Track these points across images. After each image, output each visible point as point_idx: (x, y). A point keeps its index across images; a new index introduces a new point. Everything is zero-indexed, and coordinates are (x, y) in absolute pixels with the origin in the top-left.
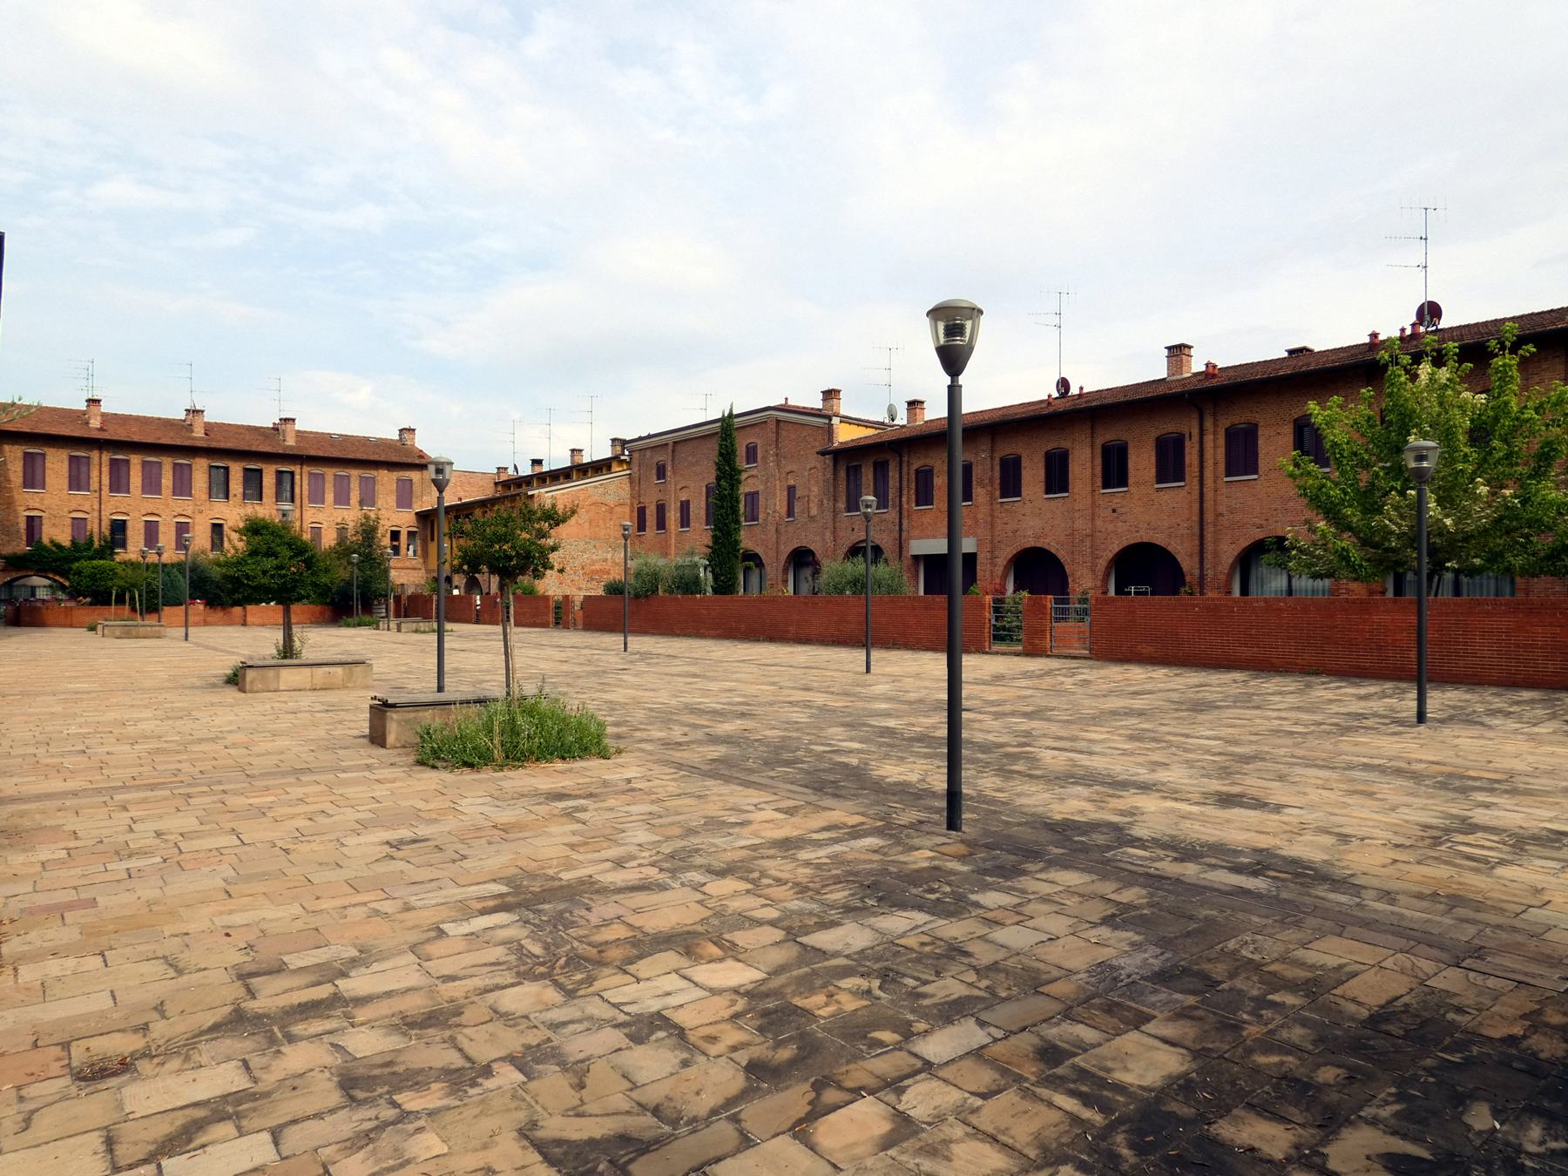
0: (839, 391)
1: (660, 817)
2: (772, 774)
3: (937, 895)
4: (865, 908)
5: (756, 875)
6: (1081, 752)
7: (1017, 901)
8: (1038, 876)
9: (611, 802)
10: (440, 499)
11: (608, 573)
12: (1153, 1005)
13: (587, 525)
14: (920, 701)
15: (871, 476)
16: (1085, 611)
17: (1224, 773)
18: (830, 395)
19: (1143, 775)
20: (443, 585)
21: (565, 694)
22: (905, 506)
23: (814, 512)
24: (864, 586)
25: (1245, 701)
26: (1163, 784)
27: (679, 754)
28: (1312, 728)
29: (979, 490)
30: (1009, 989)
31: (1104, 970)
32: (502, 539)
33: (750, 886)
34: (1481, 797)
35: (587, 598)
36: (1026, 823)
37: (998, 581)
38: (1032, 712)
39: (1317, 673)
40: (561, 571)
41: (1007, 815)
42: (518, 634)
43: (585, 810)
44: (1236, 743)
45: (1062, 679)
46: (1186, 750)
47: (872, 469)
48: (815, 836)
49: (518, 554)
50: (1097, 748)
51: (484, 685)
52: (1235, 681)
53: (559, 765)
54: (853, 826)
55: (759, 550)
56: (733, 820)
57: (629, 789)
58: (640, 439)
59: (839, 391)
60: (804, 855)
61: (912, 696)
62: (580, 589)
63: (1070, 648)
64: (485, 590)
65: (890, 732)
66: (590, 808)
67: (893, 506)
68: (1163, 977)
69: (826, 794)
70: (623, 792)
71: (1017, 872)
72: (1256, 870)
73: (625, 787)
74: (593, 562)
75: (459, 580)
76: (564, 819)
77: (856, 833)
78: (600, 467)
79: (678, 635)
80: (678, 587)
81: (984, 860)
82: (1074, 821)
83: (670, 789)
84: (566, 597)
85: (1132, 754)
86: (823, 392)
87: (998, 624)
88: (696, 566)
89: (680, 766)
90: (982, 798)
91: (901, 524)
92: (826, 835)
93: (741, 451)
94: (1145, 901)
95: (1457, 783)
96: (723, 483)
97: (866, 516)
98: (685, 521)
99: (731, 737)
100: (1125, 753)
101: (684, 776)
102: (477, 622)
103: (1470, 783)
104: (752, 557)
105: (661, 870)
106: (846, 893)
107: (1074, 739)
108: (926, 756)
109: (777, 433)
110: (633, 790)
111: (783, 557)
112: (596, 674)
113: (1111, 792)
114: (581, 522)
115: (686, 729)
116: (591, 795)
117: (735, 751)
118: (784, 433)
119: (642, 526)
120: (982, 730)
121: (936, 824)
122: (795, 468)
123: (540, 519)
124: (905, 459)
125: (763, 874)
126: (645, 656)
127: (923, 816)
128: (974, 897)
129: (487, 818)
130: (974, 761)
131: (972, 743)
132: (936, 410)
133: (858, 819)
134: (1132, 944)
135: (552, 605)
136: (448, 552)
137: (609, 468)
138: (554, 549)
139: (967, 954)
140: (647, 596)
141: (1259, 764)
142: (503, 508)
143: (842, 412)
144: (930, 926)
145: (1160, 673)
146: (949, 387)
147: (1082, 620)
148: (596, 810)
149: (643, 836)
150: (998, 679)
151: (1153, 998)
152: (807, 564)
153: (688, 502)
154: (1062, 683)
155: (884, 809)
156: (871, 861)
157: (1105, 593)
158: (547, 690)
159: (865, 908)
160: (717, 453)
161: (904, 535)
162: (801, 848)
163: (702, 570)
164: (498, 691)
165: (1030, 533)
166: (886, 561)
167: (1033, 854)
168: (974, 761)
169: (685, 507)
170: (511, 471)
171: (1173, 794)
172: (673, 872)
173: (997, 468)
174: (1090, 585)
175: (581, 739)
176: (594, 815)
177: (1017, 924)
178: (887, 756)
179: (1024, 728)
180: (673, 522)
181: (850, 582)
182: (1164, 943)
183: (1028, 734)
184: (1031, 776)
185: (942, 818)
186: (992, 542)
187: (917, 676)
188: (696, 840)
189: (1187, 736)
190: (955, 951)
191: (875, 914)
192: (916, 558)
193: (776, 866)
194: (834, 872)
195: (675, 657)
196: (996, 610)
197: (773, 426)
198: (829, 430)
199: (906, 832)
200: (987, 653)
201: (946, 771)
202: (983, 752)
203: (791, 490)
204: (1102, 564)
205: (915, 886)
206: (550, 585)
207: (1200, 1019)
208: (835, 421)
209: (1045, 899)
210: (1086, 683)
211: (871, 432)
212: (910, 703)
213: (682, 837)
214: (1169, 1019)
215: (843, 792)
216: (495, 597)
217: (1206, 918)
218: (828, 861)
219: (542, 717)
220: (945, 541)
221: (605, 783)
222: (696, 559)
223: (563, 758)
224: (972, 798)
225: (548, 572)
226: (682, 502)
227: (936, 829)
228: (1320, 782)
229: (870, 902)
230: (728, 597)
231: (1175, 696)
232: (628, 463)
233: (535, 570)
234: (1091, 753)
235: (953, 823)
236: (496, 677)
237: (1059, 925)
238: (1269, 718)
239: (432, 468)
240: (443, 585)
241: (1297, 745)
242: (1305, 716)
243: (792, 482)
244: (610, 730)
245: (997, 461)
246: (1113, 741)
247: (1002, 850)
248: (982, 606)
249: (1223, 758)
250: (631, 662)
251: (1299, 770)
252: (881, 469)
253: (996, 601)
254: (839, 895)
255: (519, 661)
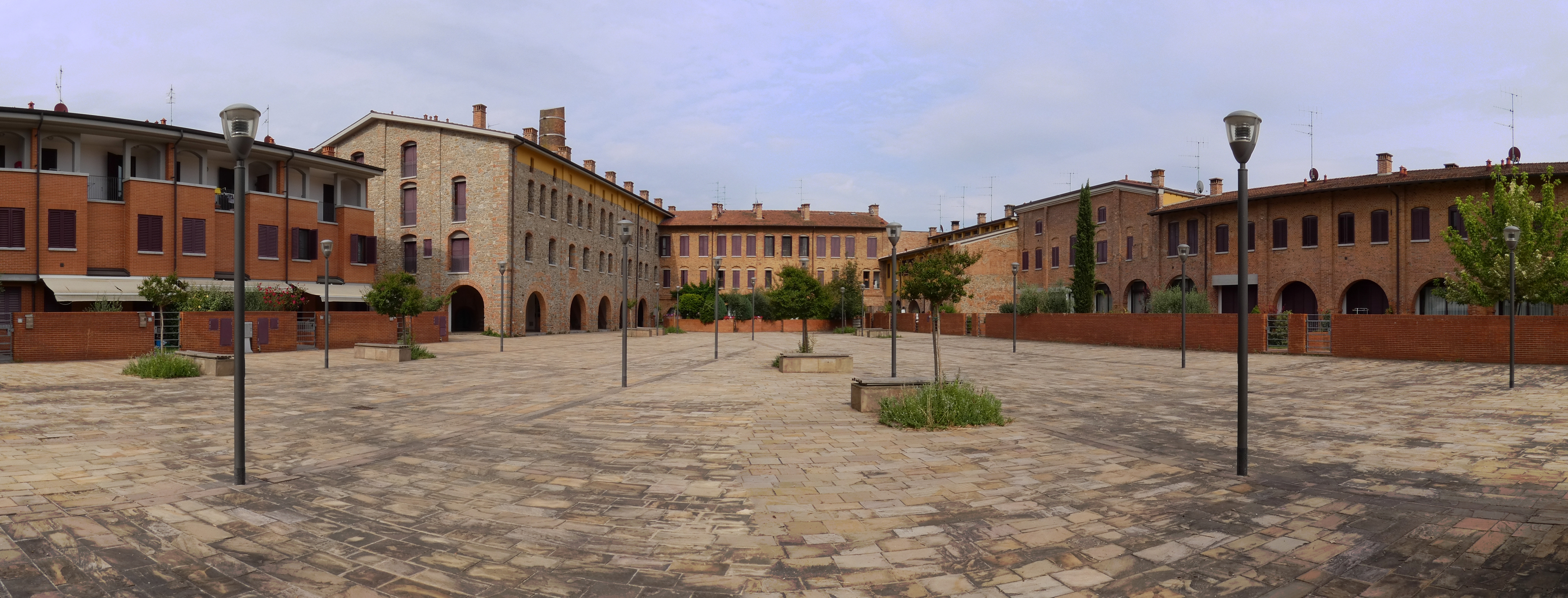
0: (1163, 171)
1: (1038, 467)
2: (1116, 438)
3: (1231, 520)
4: (1181, 531)
5: (1105, 509)
6: (1325, 418)
7: (1284, 520)
8: (1298, 502)
9: (1005, 456)
10: (894, 250)
11: (1003, 298)
12: (1368, 579)
13: (988, 265)
14: (1219, 387)
15: (1185, 230)
16: (1328, 325)
17: (1411, 426)
18: (1157, 173)
19: (1364, 430)
20: (896, 307)
21: (973, 381)
22: (1209, 252)
23: (1146, 255)
24: (1181, 307)
25: (1422, 380)
26: (1375, 436)
27: (1051, 424)
28: (1458, 394)
29: (1259, 241)
30: (1278, 580)
31: (1339, 561)
32: (932, 275)
33: (1100, 517)
34: (1538, 426)
35: (988, 315)
36: (1290, 468)
37: (1272, 304)
38: (1294, 393)
39: (1461, 361)
40: (971, 297)
41: (1278, 463)
42: (944, 340)
43: (987, 460)
44: (1417, 406)
45: (1312, 369)
46: (1389, 413)
47: (1186, 226)
48: (1146, 482)
49: (943, 286)
50: (1335, 415)
51: (921, 373)
52: (1417, 368)
53: (970, 429)
54: (1172, 475)
55: (1107, 282)
56: (1088, 470)
57: (1016, 447)
58: (1025, 205)
59: (1163, 171)
60: (1138, 495)
61: (1214, 383)
62: (984, 309)
63: (1319, 349)
64: (922, 310)
65: (1198, 408)
66: (991, 459)
67: (1201, 252)
68: (1374, 560)
69: (1154, 452)
70: (1013, 449)
71: (1285, 501)
72: (1426, 485)
73: (1013, 445)
74: (993, 291)
75: (905, 303)
76: (973, 466)
77: (1175, 479)
78: (997, 225)
79: (1051, 341)
80: (1051, 308)
81: (1262, 494)
82: (1320, 464)
83: (1045, 448)
84: (974, 315)
85: (1357, 417)
86: (1152, 172)
87: (1272, 333)
88: (1063, 293)
89: (1052, 432)
90: (1261, 452)
91: (1206, 264)
92: (1154, 481)
93: (1095, 213)
94: (1363, 512)
95: (1528, 420)
96: (1082, 235)
97: (1182, 257)
98: (1055, 262)
99: (1087, 412)
100: (1352, 417)
101: (1055, 439)
102: (917, 331)
103: (1534, 419)
104: (1102, 286)
105: (1039, 504)
106: (1168, 521)
107: (1320, 409)
108: (1223, 425)
109: (1120, 200)
110: (1019, 448)
111: (1124, 287)
112: (994, 367)
113: (1344, 443)
114: (984, 263)
115: (1056, 407)
116: (991, 451)
117: (1091, 423)
118: (1125, 200)
119: (1025, 265)
120: (1261, 406)
121: (1230, 471)
122: (1132, 224)
123: (957, 262)
124: (1209, 219)
125: (1110, 508)
126: (1028, 355)
127: (1220, 466)
128: (1255, 520)
129: (923, 462)
130: (1255, 427)
131: (1254, 415)
132: (1230, 186)
133: (1176, 469)
134: (1356, 541)
135: (965, 320)
136: (898, 284)
137: (1003, 226)
138: (966, 282)
139: (1250, 559)
140: (1029, 314)
141: (1430, 419)
142: (933, 255)
143: (1166, 186)
144: (1225, 542)
145: (1374, 364)
146: (1239, 170)
147: (1326, 330)
148: (994, 461)
149: (1026, 480)
150: (1272, 371)
151: (1368, 574)
152: (1141, 292)
153: (1057, 248)
154: (1313, 372)
155: (1194, 462)
156: (1185, 499)
157: (1340, 312)
158: (961, 378)
159: (1181, 531)
160: (1077, 214)
161: (1208, 271)
162: (1136, 490)
163: (1067, 296)
164: (931, 378)
165: (1293, 271)
166: (1196, 290)
167: (1294, 488)
168: (1255, 427)
169: (1055, 252)
170: (938, 230)
171: (1382, 442)
172: (1047, 506)
173: (1271, 227)
174: (1331, 307)
175: (984, 411)
176: (993, 464)
177: (1284, 536)
178: (1196, 425)
179: (1289, 403)
180: (1047, 263)
181: (1170, 305)
182: (1375, 538)
183: (1291, 407)
184: (1293, 436)
185: (1234, 467)
186: (1268, 278)
187: (1217, 369)
188: (1062, 484)
189: (1390, 404)
190: (1243, 557)
191: (1188, 535)
192: (1216, 287)
193: (1119, 503)
194: (1159, 507)
195: (1048, 356)
196: (1271, 324)
197: (1117, 195)
198: (1157, 198)
199: (1209, 477)
200: (1264, 353)
201: (1236, 434)
202: (1262, 421)
203: (1130, 240)
204: (1339, 293)
205: (1216, 515)
206: (964, 307)
207: (1396, 582)
208: (1161, 191)
209: (1302, 518)
210: (1328, 372)
211: (1186, 200)
212: (1212, 388)
213: (1053, 482)
214: (1378, 586)
215: (1166, 451)
216: (928, 315)
217: (1400, 518)
218: (1155, 499)
219: (959, 396)
220: (1236, 276)
221: (1001, 443)
222: (1063, 288)
223: (973, 425)
224: (1254, 453)
225: (963, 298)
226: (1053, 249)
227: (1230, 475)
228: (1462, 427)
229: (1184, 527)
230: (1085, 315)
231: (1382, 379)
232: (1017, 222)
233: (954, 296)
234: (1331, 418)
235: (1241, 470)
236: (929, 368)
237: (1310, 534)
238: (1435, 390)
239: (889, 230)
240: (896, 307)
241: (1450, 405)
242: (1455, 388)
243: (1130, 234)
244: (1004, 406)
245: (1271, 222)
246: (1345, 409)
247: (1273, 486)
248: (1261, 321)
249: (1410, 416)
250: (1018, 359)
251: (1451, 420)
252: (1192, 226)
253: (1270, 317)
254: (1162, 523)
255: (943, 357)
